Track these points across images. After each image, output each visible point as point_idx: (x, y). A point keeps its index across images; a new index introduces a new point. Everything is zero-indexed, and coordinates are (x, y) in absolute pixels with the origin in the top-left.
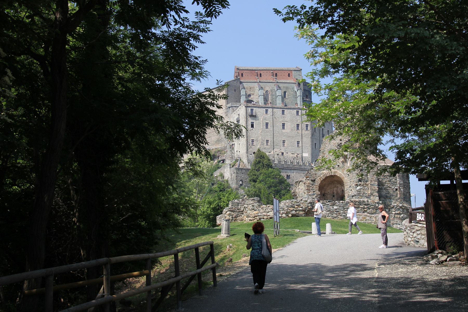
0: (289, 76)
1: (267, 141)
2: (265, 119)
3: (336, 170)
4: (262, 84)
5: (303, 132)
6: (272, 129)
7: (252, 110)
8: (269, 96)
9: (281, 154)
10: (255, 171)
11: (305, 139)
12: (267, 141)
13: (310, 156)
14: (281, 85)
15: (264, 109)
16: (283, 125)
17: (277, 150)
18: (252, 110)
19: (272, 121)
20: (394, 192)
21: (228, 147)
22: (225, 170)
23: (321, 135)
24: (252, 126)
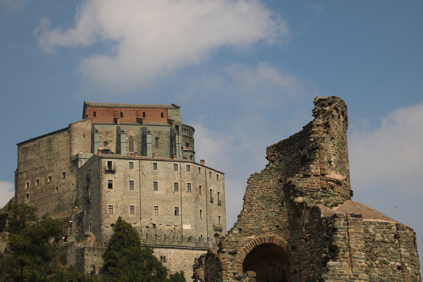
0: (162, 116)
1: (132, 207)
2: (129, 175)
3: (273, 235)
5: (184, 194)
6: (138, 190)
7: (110, 163)
8: (134, 144)
9: (151, 226)
11: (186, 205)
14: (150, 128)
15: (128, 162)
17: (146, 221)
18: (110, 163)
19: (138, 179)
20: (394, 271)
23: (209, 199)
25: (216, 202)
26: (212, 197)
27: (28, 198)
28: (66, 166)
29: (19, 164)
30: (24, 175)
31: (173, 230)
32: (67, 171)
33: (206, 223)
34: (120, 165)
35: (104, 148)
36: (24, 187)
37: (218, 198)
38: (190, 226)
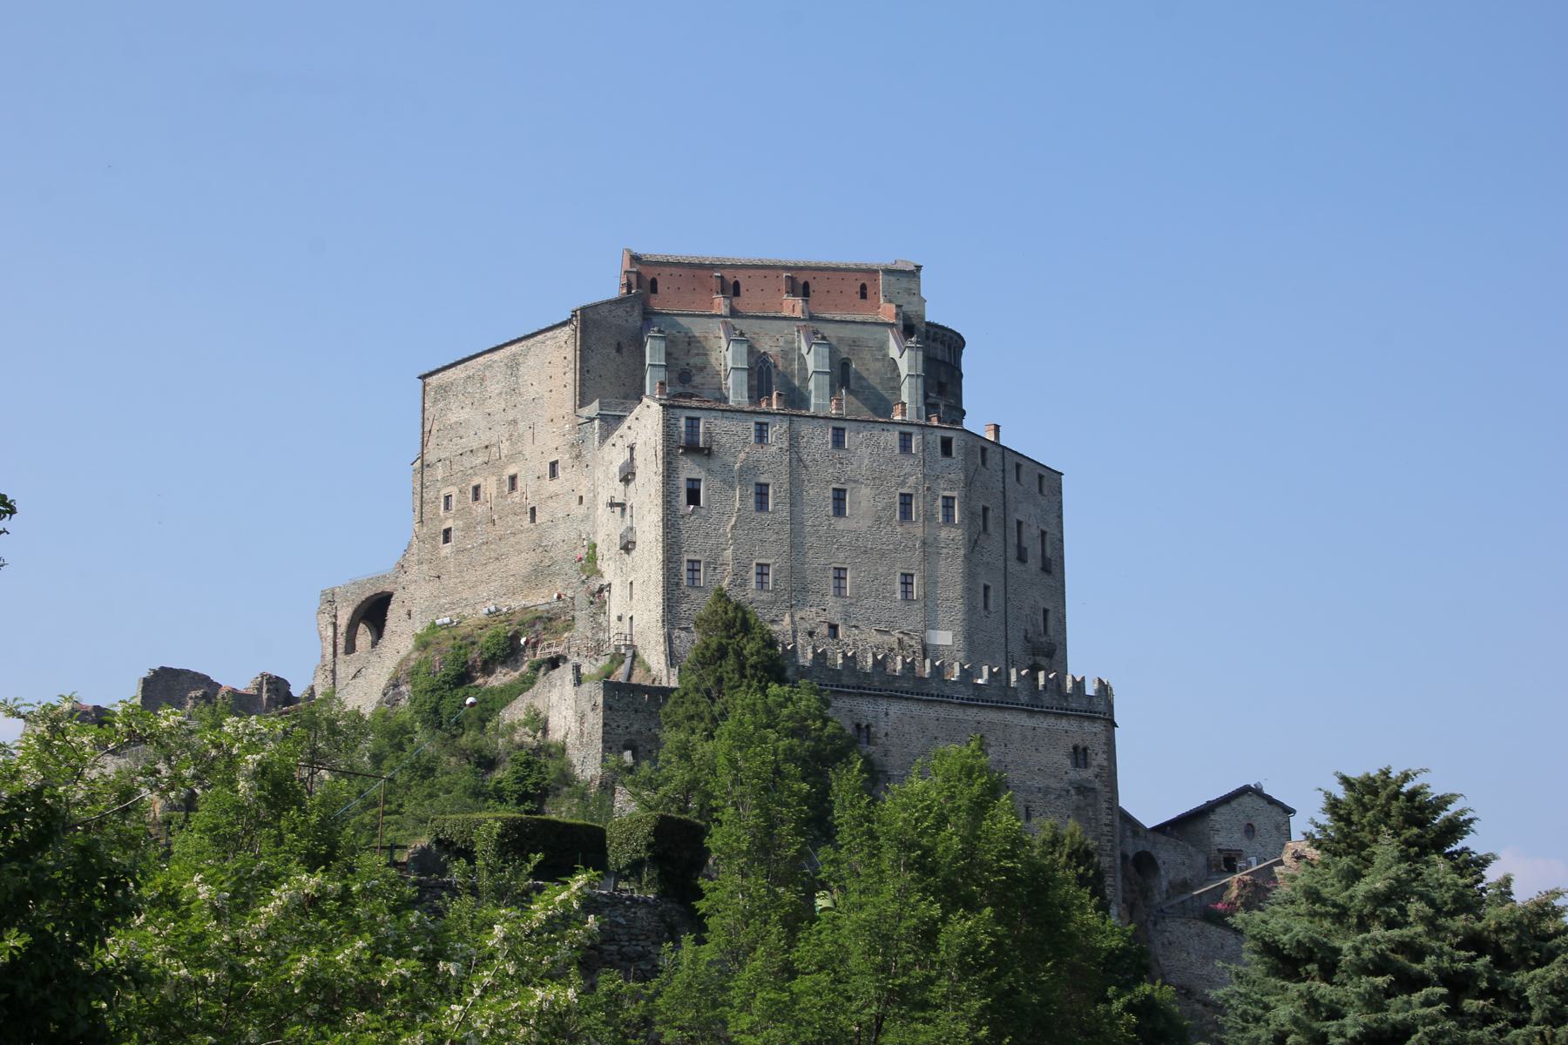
0: (864, 296)
1: (762, 570)
4: (740, 324)
6: (785, 514)
7: (693, 422)
9: (824, 630)
10: (698, 697)
12: (762, 570)
13: (961, 643)
14: (828, 330)
16: (839, 496)
19: (785, 478)
21: (582, 598)
22: (554, 697)
23: (1012, 552)
24: (693, 497)
25: (1034, 563)
26: (1025, 544)
27: (447, 540)
28: (559, 441)
29: (425, 435)
30: (440, 472)
31: (896, 646)
32: (564, 458)
33: (1002, 627)
34: (726, 433)
35: (680, 389)
36: (438, 507)
37: (1043, 550)
38: (950, 634)
